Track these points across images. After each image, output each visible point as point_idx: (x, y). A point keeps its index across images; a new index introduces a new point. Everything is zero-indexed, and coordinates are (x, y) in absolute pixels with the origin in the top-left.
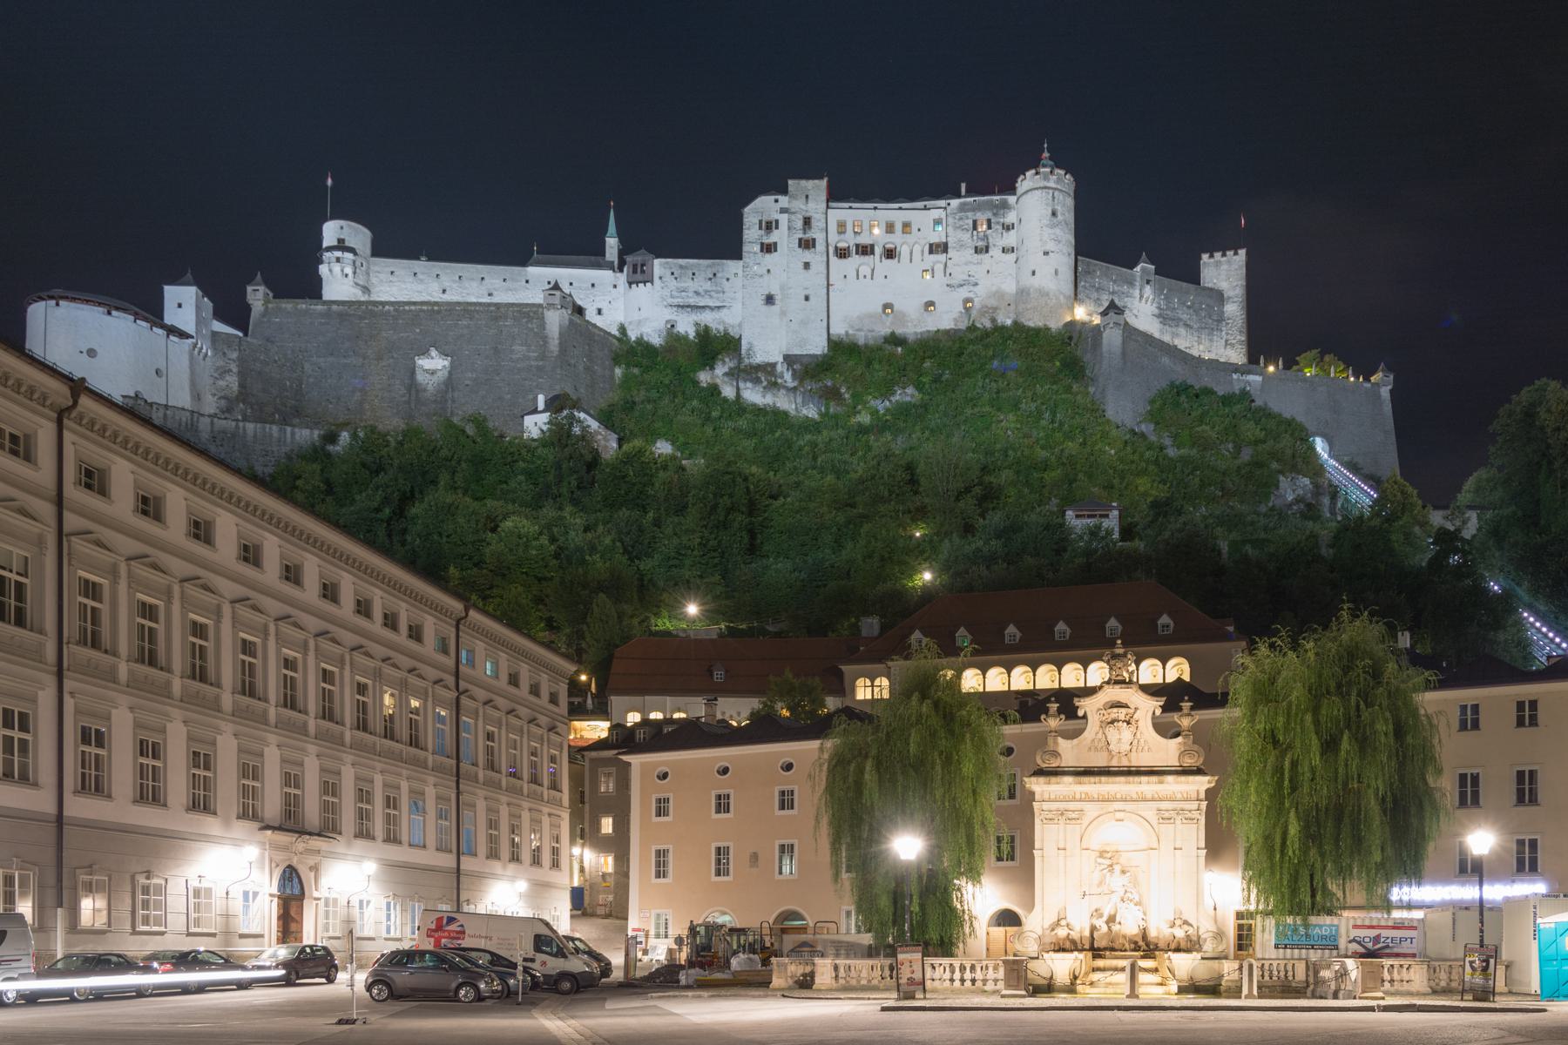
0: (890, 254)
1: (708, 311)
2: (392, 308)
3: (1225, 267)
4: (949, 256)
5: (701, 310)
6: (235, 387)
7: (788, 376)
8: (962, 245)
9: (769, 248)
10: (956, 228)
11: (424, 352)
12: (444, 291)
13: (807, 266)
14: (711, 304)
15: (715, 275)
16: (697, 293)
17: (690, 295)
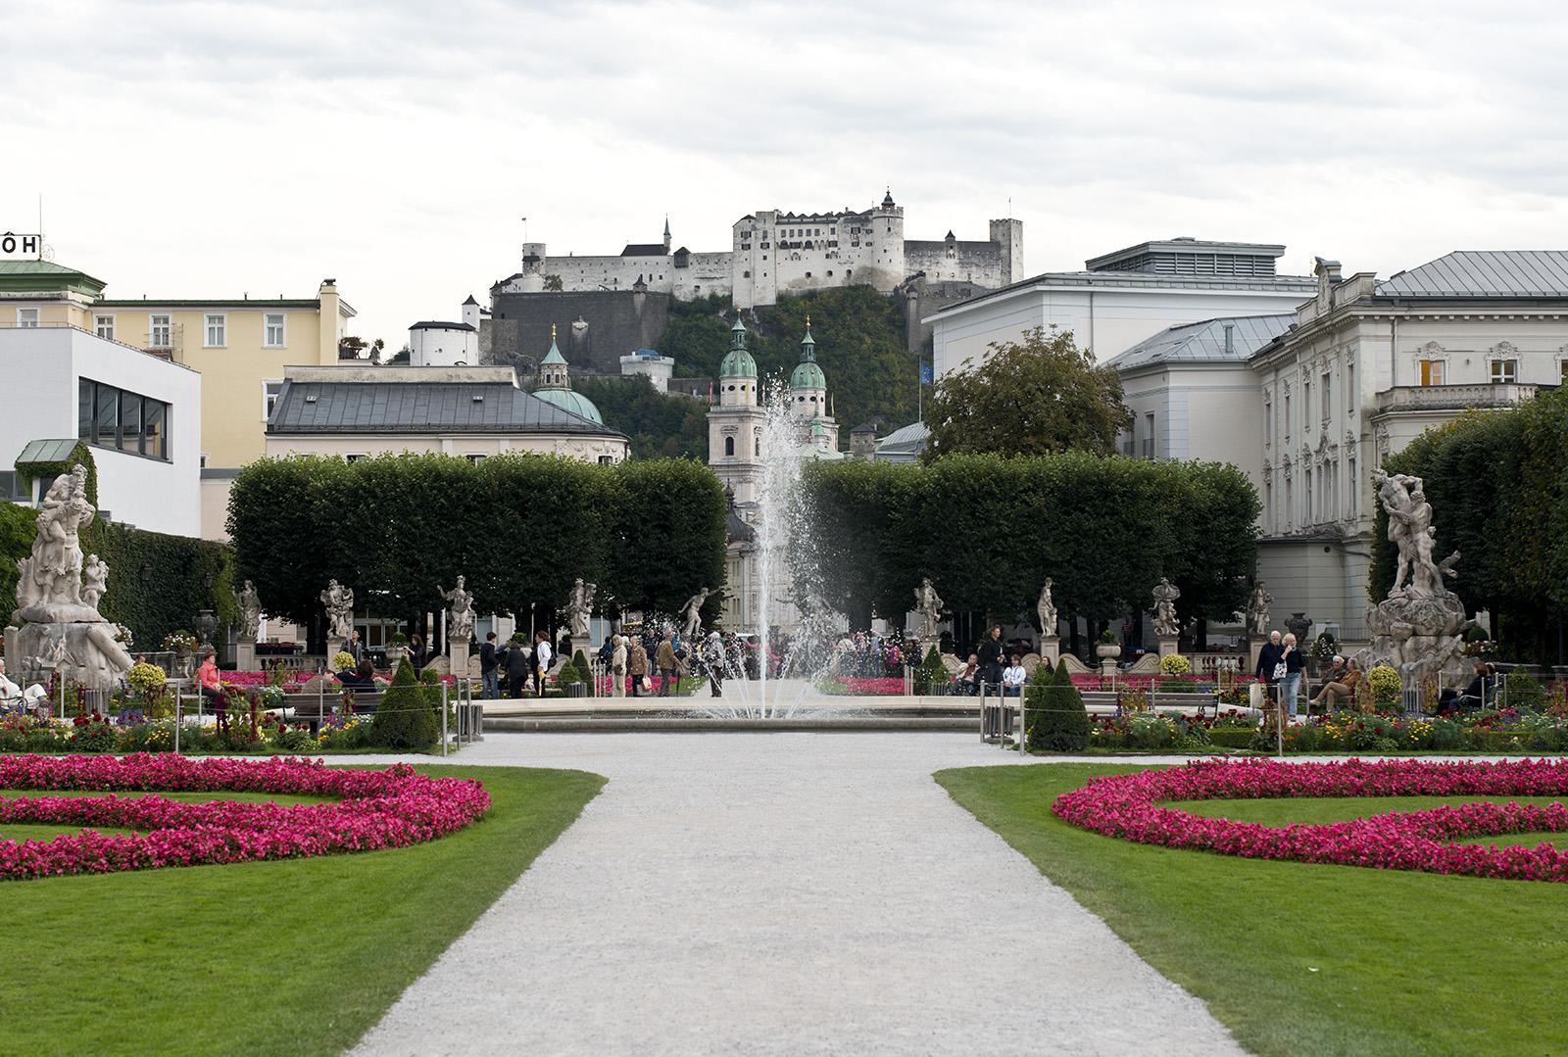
0: (809, 245)
3: (1001, 228)
6: (490, 345)
11: (578, 320)
13: (765, 258)
16: (710, 270)
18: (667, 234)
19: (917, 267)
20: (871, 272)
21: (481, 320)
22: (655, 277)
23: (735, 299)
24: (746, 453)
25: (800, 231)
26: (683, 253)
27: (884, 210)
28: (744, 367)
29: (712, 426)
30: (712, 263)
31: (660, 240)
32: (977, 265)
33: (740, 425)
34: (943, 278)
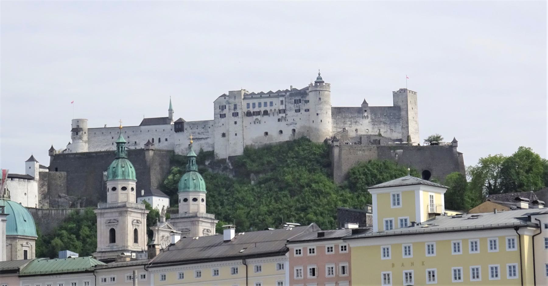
0: (266, 113)
1: (203, 140)
2: (95, 154)
3: (400, 97)
4: (287, 114)
5: (201, 140)
6: (46, 190)
7: (230, 164)
8: (291, 109)
9: (223, 116)
10: (288, 103)
12: (113, 138)
13: (236, 123)
14: (204, 137)
15: (205, 126)
16: (199, 133)
17: (197, 134)
18: (171, 111)
19: (342, 125)
21: (40, 173)
22: (163, 140)
23: (216, 151)
24: (125, 239)
25: (260, 104)
27: (316, 86)
28: (123, 172)
32: (384, 123)
33: (120, 219)
34: (360, 133)
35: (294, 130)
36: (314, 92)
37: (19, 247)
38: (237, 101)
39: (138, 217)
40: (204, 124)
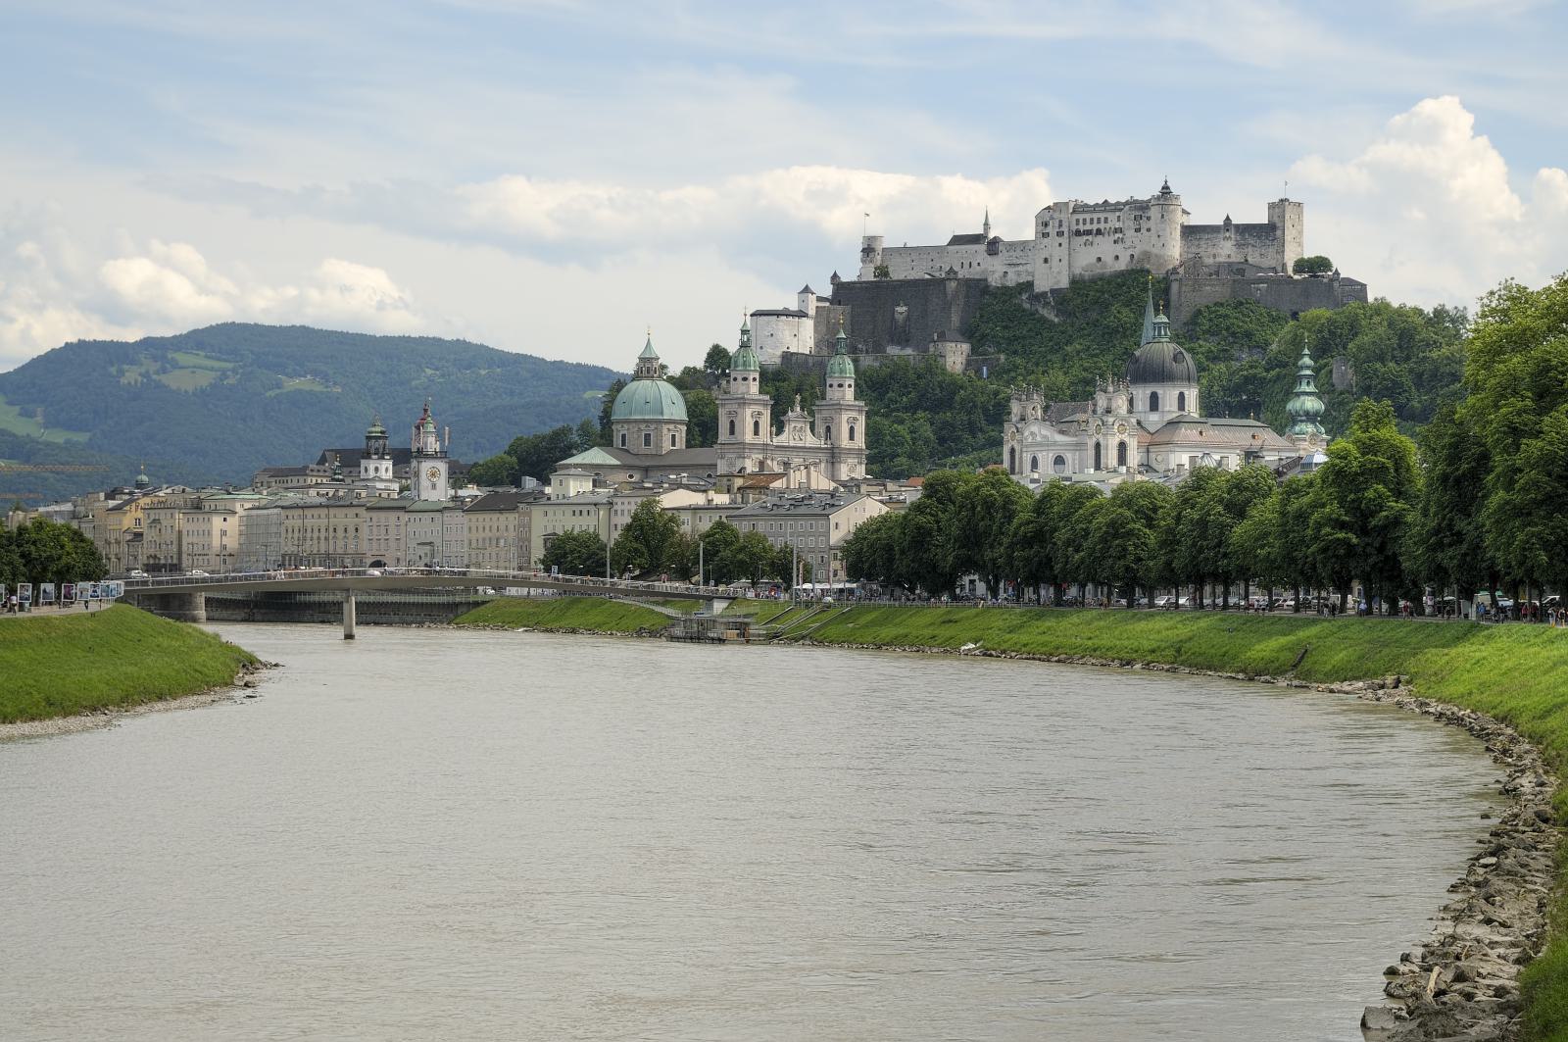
0: (1099, 232)
3: (1277, 210)
9: (1045, 235)
11: (899, 305)
13: (1060, 245)
18: (986, 224)
19: (1194, 250)
20: (1147, 255)
21: (817, 307)
22: (974, 264)
23: (1036, 283)
24: (744, 434)
25: (1092, 220)
26: (995, 241)
29: (720, 410)
30: (1018, 250)
31: (980, 231)
32: (1253, 246)
35: (1133, 256)
36: (1157, 207)
37: (665, 431)
38: (1063, 216)
39: (760, 408)
40: (1023, 245)
